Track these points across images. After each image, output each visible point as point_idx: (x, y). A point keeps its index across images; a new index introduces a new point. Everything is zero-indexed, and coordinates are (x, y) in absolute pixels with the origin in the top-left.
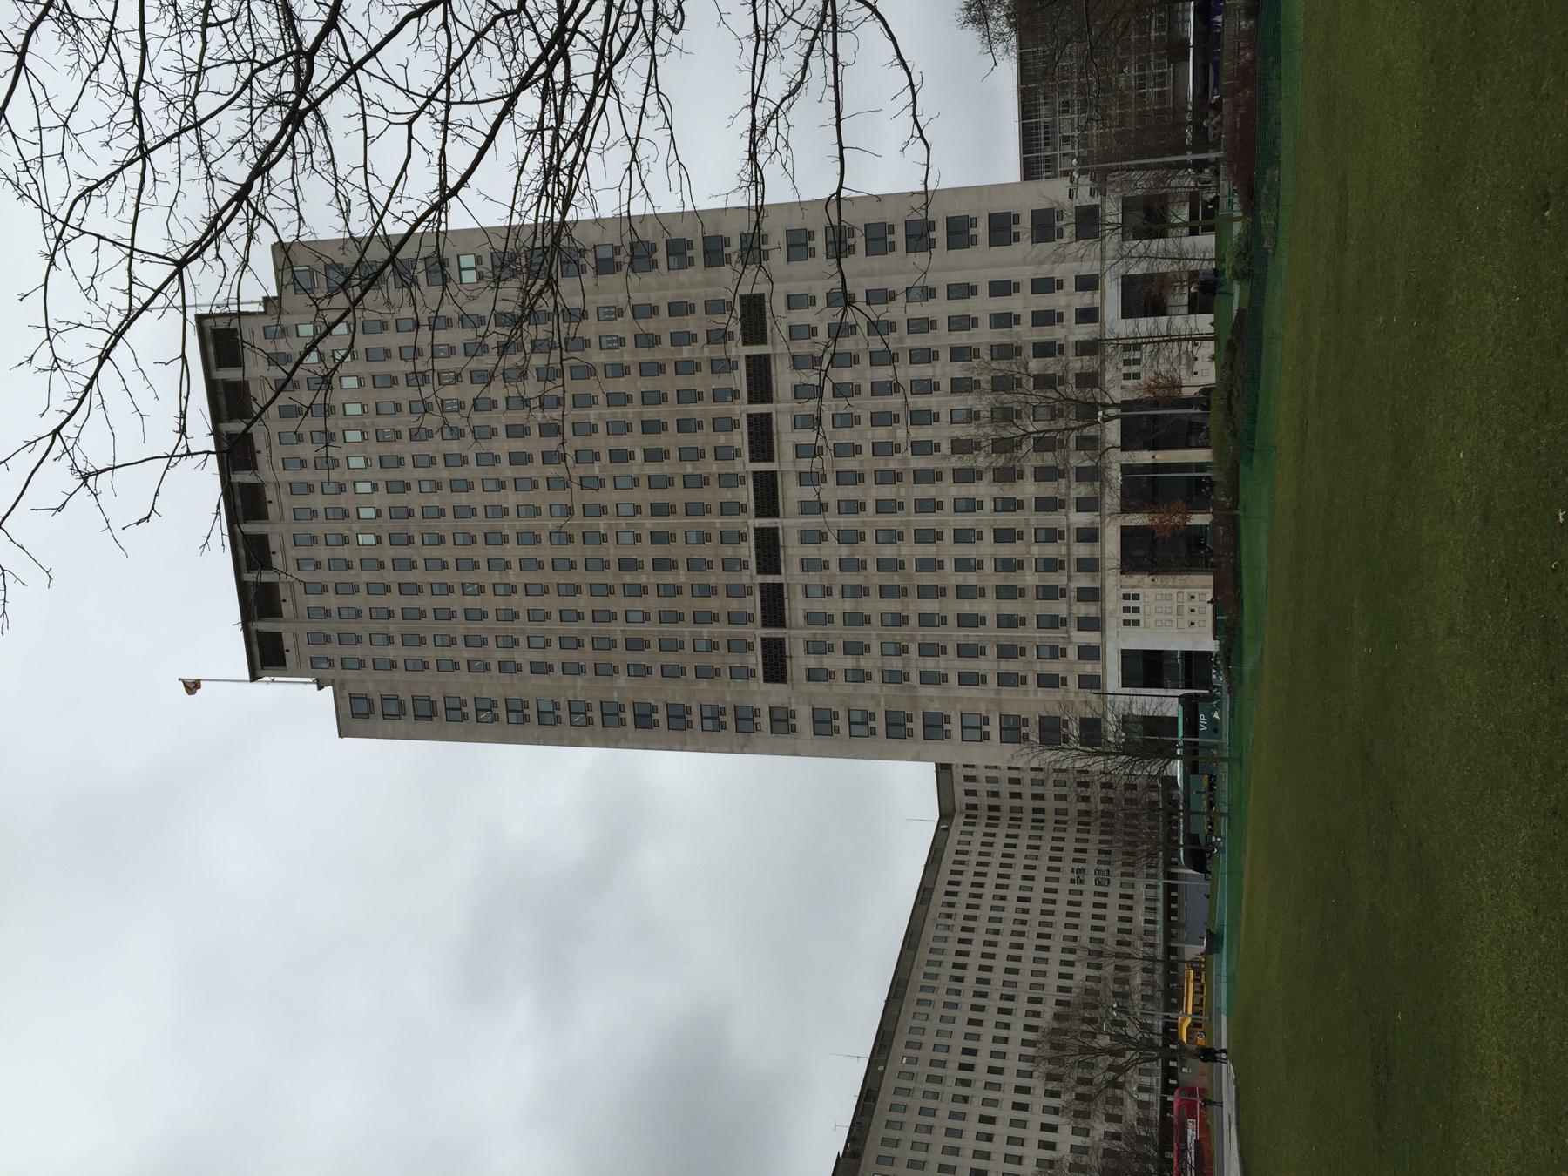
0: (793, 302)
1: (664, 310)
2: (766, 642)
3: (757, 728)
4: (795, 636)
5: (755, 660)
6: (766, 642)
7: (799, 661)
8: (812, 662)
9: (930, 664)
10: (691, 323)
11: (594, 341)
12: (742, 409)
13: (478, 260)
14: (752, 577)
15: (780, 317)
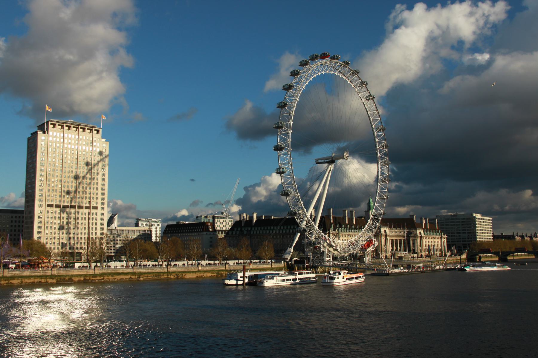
0: (96, 214)
1: (97, 196)
2: (53, 205)
3: (40, 202)
4: (54, 209)
5: (50, 203)
6: (53, 205)
7: (50, 209)
8: (50, 211)
9: (49, 227)
10: (95, 199)
11: (94, 186)
12: (84, 205)
13: (105, 172)
14: (62, 204)
15: (94, 211)
